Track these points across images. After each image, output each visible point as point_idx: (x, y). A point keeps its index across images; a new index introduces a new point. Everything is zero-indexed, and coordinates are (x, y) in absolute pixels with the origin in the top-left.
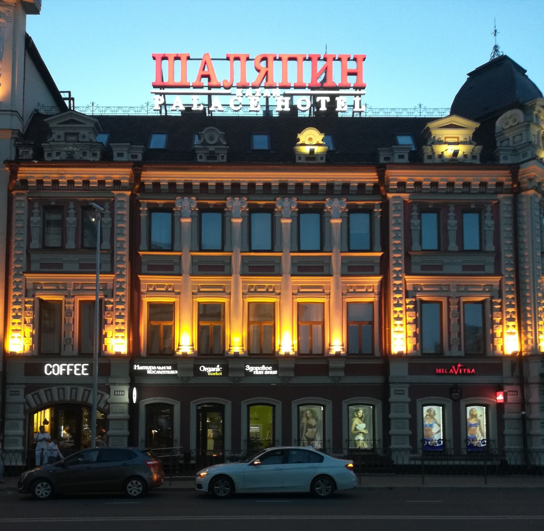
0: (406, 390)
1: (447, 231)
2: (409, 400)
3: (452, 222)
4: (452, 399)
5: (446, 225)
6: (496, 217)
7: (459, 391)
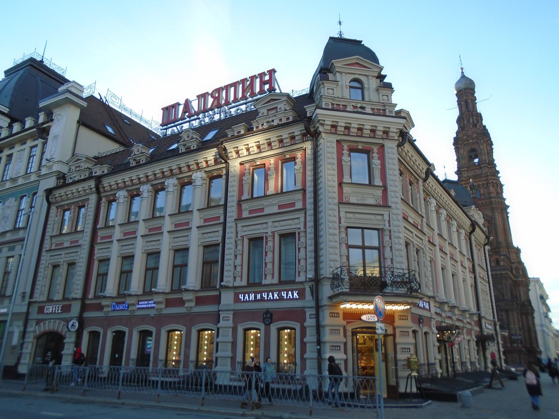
7: (269, 316)
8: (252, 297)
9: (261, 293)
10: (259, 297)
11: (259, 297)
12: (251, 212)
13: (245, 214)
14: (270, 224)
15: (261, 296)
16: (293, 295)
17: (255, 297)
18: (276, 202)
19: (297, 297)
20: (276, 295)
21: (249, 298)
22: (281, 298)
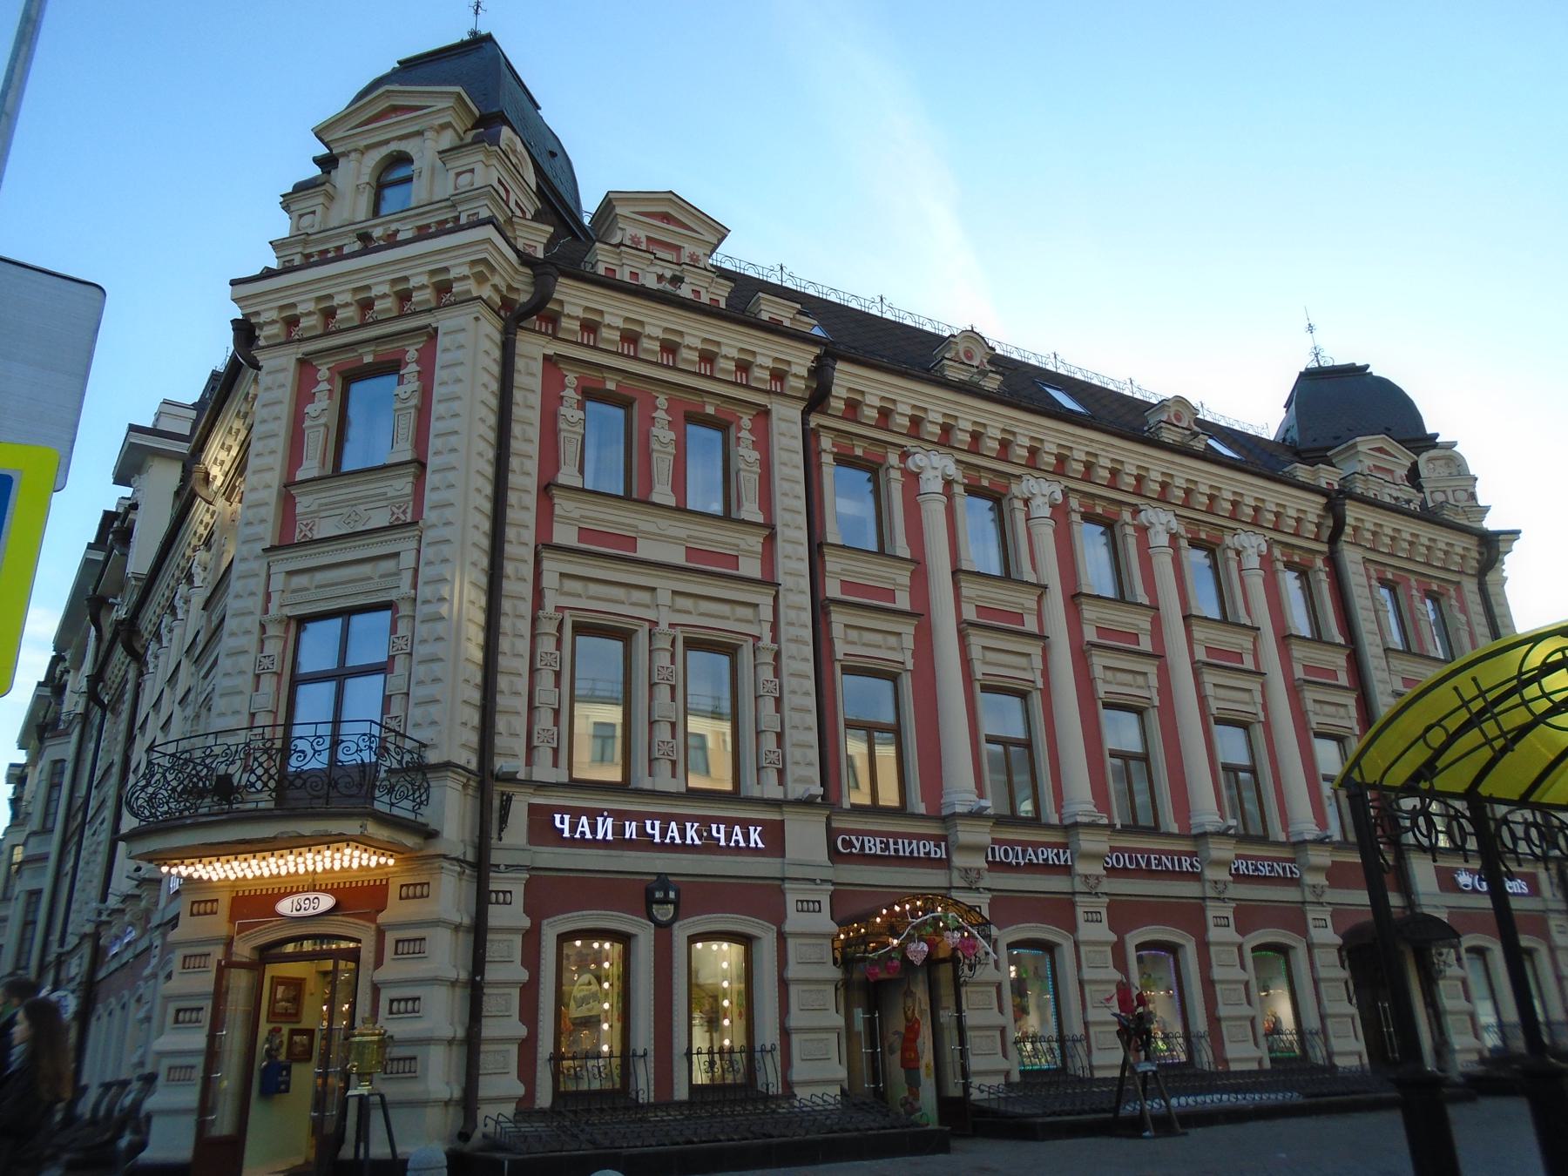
0: (518, 891)
2: (526, 923)
3: (663, 434)
4: (651, 918)
5: (647, 438)
6: (763, 444)
7: (672, 895)
8: (606, 828)
9: (640, 818)
10: (631, 830)
11: (631, 830)
12: (584, 534)
13: (564, 535)
14: (664, 597)
15: (641, 830)
16: (747, 838)
17: (619, 830)
18: (683, 534)
19: (760, 845)
20: (691, 833)
21: (594, 830)
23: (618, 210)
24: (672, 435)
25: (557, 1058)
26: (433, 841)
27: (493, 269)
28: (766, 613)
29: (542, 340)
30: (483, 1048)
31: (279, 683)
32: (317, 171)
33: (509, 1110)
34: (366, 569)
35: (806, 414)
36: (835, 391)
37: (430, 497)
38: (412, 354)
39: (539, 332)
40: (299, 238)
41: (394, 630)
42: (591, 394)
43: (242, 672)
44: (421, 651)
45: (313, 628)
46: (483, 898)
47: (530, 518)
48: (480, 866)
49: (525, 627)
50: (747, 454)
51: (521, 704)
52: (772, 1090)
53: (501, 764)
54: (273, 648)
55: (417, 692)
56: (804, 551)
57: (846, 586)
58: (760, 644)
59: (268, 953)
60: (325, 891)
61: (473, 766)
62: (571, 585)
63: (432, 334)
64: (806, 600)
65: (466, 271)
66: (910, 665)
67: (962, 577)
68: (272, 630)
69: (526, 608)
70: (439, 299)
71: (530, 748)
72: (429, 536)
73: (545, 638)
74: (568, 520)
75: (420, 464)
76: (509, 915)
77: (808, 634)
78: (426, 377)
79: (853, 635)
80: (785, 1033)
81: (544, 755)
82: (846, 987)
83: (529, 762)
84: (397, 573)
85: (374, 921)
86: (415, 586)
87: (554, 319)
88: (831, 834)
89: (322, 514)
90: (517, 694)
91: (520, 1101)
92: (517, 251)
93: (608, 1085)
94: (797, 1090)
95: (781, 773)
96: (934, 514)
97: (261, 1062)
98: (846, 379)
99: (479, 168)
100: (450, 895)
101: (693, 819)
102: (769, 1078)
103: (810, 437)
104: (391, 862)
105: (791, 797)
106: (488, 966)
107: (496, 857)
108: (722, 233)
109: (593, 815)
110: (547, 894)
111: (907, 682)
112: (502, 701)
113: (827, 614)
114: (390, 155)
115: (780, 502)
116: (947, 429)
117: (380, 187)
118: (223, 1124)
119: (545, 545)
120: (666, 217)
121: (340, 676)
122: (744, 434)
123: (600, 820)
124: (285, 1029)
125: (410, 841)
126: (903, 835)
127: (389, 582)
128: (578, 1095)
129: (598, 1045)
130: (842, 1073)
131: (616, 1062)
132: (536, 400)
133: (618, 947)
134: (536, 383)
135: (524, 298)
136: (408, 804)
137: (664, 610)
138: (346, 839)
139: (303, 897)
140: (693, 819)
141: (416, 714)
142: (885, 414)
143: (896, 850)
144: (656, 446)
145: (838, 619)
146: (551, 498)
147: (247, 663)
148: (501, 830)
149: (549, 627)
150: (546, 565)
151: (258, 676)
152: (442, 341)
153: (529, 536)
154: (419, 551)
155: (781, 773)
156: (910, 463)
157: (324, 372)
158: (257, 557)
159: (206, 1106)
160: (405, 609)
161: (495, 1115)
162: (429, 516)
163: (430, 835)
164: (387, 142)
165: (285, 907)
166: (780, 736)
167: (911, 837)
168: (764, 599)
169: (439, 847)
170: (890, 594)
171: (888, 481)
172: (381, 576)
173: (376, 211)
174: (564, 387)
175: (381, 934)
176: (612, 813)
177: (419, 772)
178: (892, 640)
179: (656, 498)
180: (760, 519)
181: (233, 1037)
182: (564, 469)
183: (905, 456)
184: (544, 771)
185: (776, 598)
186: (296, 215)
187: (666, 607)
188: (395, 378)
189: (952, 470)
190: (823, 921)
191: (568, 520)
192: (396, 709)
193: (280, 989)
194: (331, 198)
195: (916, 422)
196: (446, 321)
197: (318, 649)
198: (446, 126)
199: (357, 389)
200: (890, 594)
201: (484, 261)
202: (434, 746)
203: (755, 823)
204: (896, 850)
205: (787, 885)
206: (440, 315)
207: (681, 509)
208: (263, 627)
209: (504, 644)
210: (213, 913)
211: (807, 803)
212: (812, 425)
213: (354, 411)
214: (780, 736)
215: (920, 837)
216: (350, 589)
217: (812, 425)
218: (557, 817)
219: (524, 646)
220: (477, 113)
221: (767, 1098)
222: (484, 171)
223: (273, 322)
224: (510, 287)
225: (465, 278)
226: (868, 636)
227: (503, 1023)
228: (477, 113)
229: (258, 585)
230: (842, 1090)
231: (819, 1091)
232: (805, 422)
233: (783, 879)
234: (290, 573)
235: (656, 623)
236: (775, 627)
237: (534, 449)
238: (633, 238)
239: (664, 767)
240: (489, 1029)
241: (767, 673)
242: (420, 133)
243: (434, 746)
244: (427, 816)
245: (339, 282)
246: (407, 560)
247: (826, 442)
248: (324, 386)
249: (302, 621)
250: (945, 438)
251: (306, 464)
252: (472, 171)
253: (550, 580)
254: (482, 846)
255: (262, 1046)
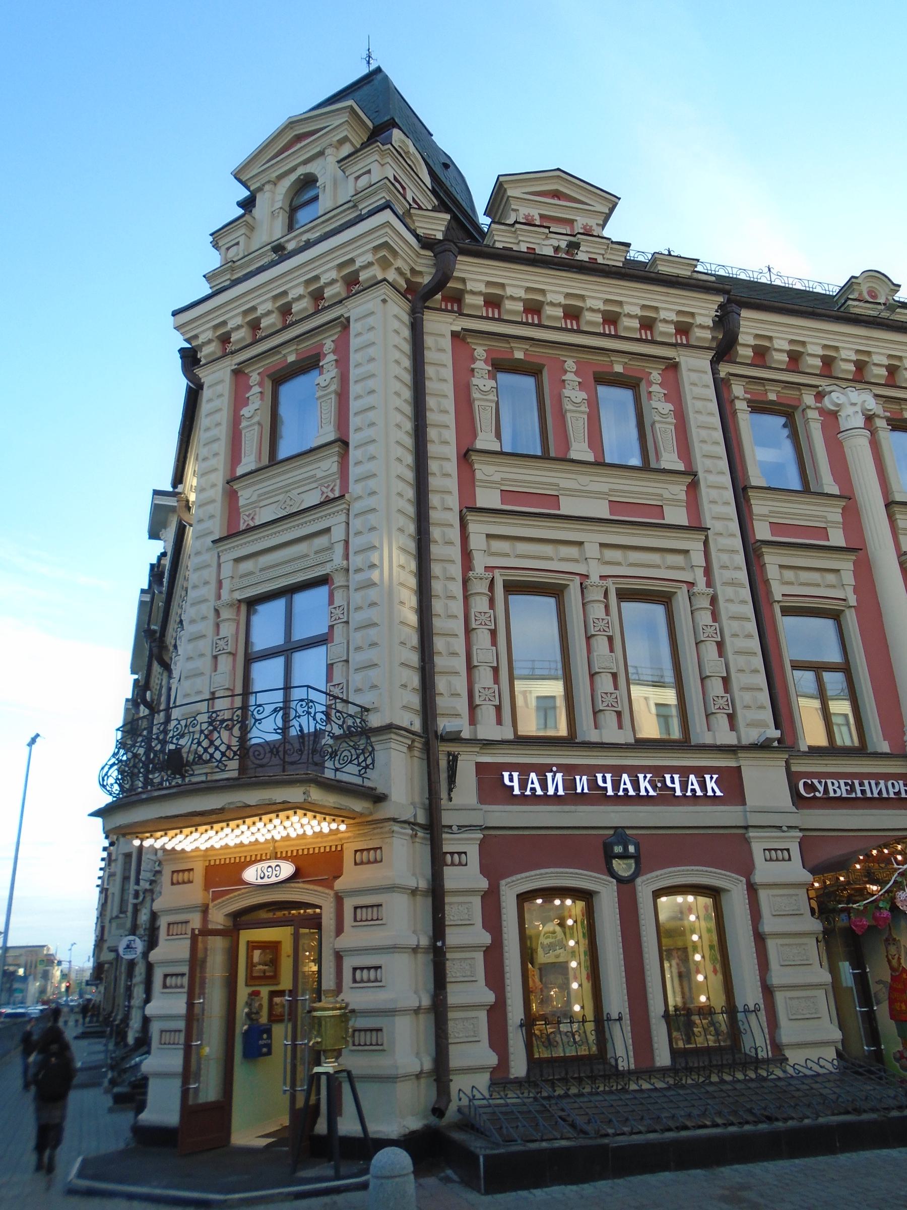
0: (473, 852)
1: (561, 415)
2: (484, 884)
3: (574, 394)
4: (612, 873)
5: (559, 400)
6: (675, 395)
7: (631, 849)
8: (556, 783)
11: (582, 784)
14: (592, 550)
15: (593, 784)
17: (570, 785)
18: (605, 488)
19: (718, 793)
20: (644, 784)
21: (544, 786)
22: (666, 797)
23: (510, 193)
24: (584, 395)
25: (529, 1022)
26: (383, 804)
27: (395, 253)
28: (698, 558)
29: (449, 318)
30: (451, 1015)
31: (234, 661)
32: (241, 211)
33: (482, 1081)
34: (302, 548)
35: (715, 362)
36: (742, 339)
37: (354, 472)
38: (329, 345)
39: (446, 310)
40: (229, 265)
41: (331, 601)
42: (500, 366)
43: (202, 655)
44: (357, 618)
45: (263, 609)
46: (437, 860)
47: (452, 484)
48: (432, 828)
49: (457, 588)
50: (660, 407)
51: (460, 664)
52: (762, 1054)
53: (444, 724)
54: (227, 630)
55: (356, 658)
56: (729, 495)
57: (775, 527)
58: (695, 589)
59: (241, 919)
60: (286, 858)
61: (417, 727)
62: (497, 545)
63: (345, 324)
64: (738, 543)
65: (370, 257)
66: (852, 601)
67: (896, 509)
68: (225, 614)
69: (456, 570)
70: (349, 290)
71: (473, 707)
72: (356, 507)
73: (478, 598)
74: (489, 484)
75: (343, 443)
76: (465, 878)
77: (743, 576)
78: (343, 363)
79: (789, 575)
80: (768, 991)
81: (487, 713)
82: (827, 936)
83: (473, 721)
84: (330, 548)
85: (332, 888)
86: (347, 557)
87: (457, 298)
88: (792, 778)
89: (260, 502)
90: (454, 654)
91: (494, 1071)
92: (417, 236)
93: (583, 1051)
94: (788, 1053)
95: (731, 718)
96: (858, 449)
97: (241, 1027)
98: (752, 326)
99: (375, 168)
100: (404, 860)
101: (645, 769)
102: (756, 1039)
103: (721, 386)
104: (343, 827)
105: (745, 742)
106: (448, 930)
107: (447, 818)
108: (612, 202)
109: (542, 770)
110: (503, 853)
111: (851, 620)
112: (440, 662)
113: (760, 556)
114: (298, 179)
115: (698, 449)
116: (860, 366)
117: (293, 211)
118: (209, 1090)
119: (469, 509)
120: (556, 194)
121: (288, 650)
122: (655, 388)
123: (549, 776)
124: (264, 991)
125: (359, 806)
126: (869, 776)
127: (323, 557)
128: (552, 1061)
129: (569, 1004)
130: (837, 1035)
131: (590, 1026)
132: (448, 373)
133: (580, 905)
134: (447, 358)
135: (426, 280)
136: (352, 768)
137: (593, 564)
138: (294, 807)
139: (265, 864)
140: (645, 769)
141: (357, 679)
142: (795, 358)
143: (863, 792)
144: (568, 406)
145: (772, 560)
146: (471, 465)
147: (205, 646)
148: (450, 790)
149: (481, 587)
150: (472, 528)
151: (215, 657)
152: (354, 327)
153: (453, 501)
154: (348, 524)
155: (731, 718)
156: (827, 403)
157: (254, 378)
158: (208, 550)
159: (188, 1074)
160: (339, 580)
161: (470, 1085)
162: (355, 489)
163: (379, 798)
164: (294, 169)
165: (250, 875)
166: (726, 681)
167: (877, 777)
168: (695, 545)
169: (386, 811)
170: (823, 532)
171: (807, 421)
172: (316, 553)
173: (291, 227)
174: (474, 360)
175: (339, 900)
176: (561, 768)
177: (362, 735)
178: (831, 578)
179: (574, 455)
180: (681, 467)
181: (214, 1000)
182: (481, 436)
183: (820, 396)
184: (488, 730)
185: (706, 543)
186: (223, 249)
187: (594, 560)
188: (316, 372)
189: (872, 404)
190: (795, 870)
191: (489, 484)
192: (338, 678)
193: (257, 954)
194: (252, 229)
195: (828, 362)
196: (355, 309)
197: (267, 628)
198: (344, 140)
199: (287, 391)
200: (823, 532)
201: (385, 245)
202: (376, 710)
203: (711, 770)
204: (863, 792)
205: (752, 834)
206: (350, 303)
207: (599, 464)
208: (217, 612)
209: (437, 606)
210: (190, 882)
211: (764, 747)
212: (722, 375)
213: (284, 411)
214: (726, 681)
215: (887, 777)
216: (288, 569)
217: (722, 375)
218: (506, 775)
219: (457, 607)
220: (370, 125)
221: (757, 1062)
222: (378, 167)
223: (210, 341)
224: (413, 270)
225: (370, 264)
226: (804, 576)
227: (469, 990)
228: (370, 125)
229: (209, 574)
230: (839, 1055)
231: (814, 1054)
232: (715, 372)
233: (746, 828)
234: (237, 560)
235: (587, 576)
236: (708, 571)
237: (450, 419)
238: (526, 217)
239: (610, 719)
240: (455, 995)
241: (705, 618)
242: (321, 154)
243: (376, 710)
244: (374, 780)
245: (260, 294)
246: (338, 533)
247: (738, 389)
248: (256, 389)
249: (252, 603)
250: (860, 375)
251: (244, 460)
252: (369, 172)
253: (477, 542)
254: (433, 808)
255: (242, 1010)
